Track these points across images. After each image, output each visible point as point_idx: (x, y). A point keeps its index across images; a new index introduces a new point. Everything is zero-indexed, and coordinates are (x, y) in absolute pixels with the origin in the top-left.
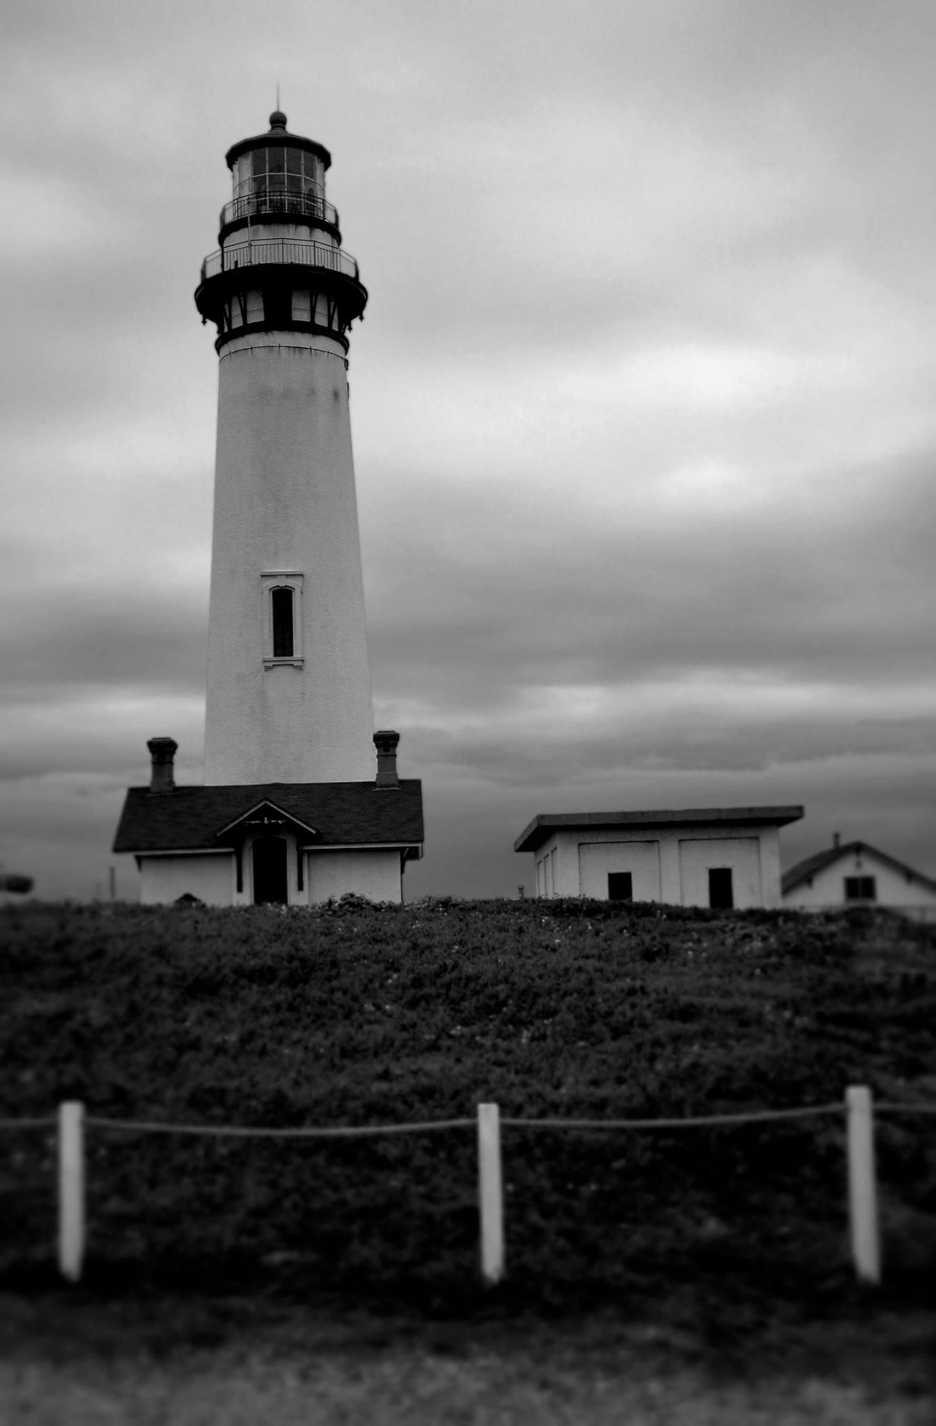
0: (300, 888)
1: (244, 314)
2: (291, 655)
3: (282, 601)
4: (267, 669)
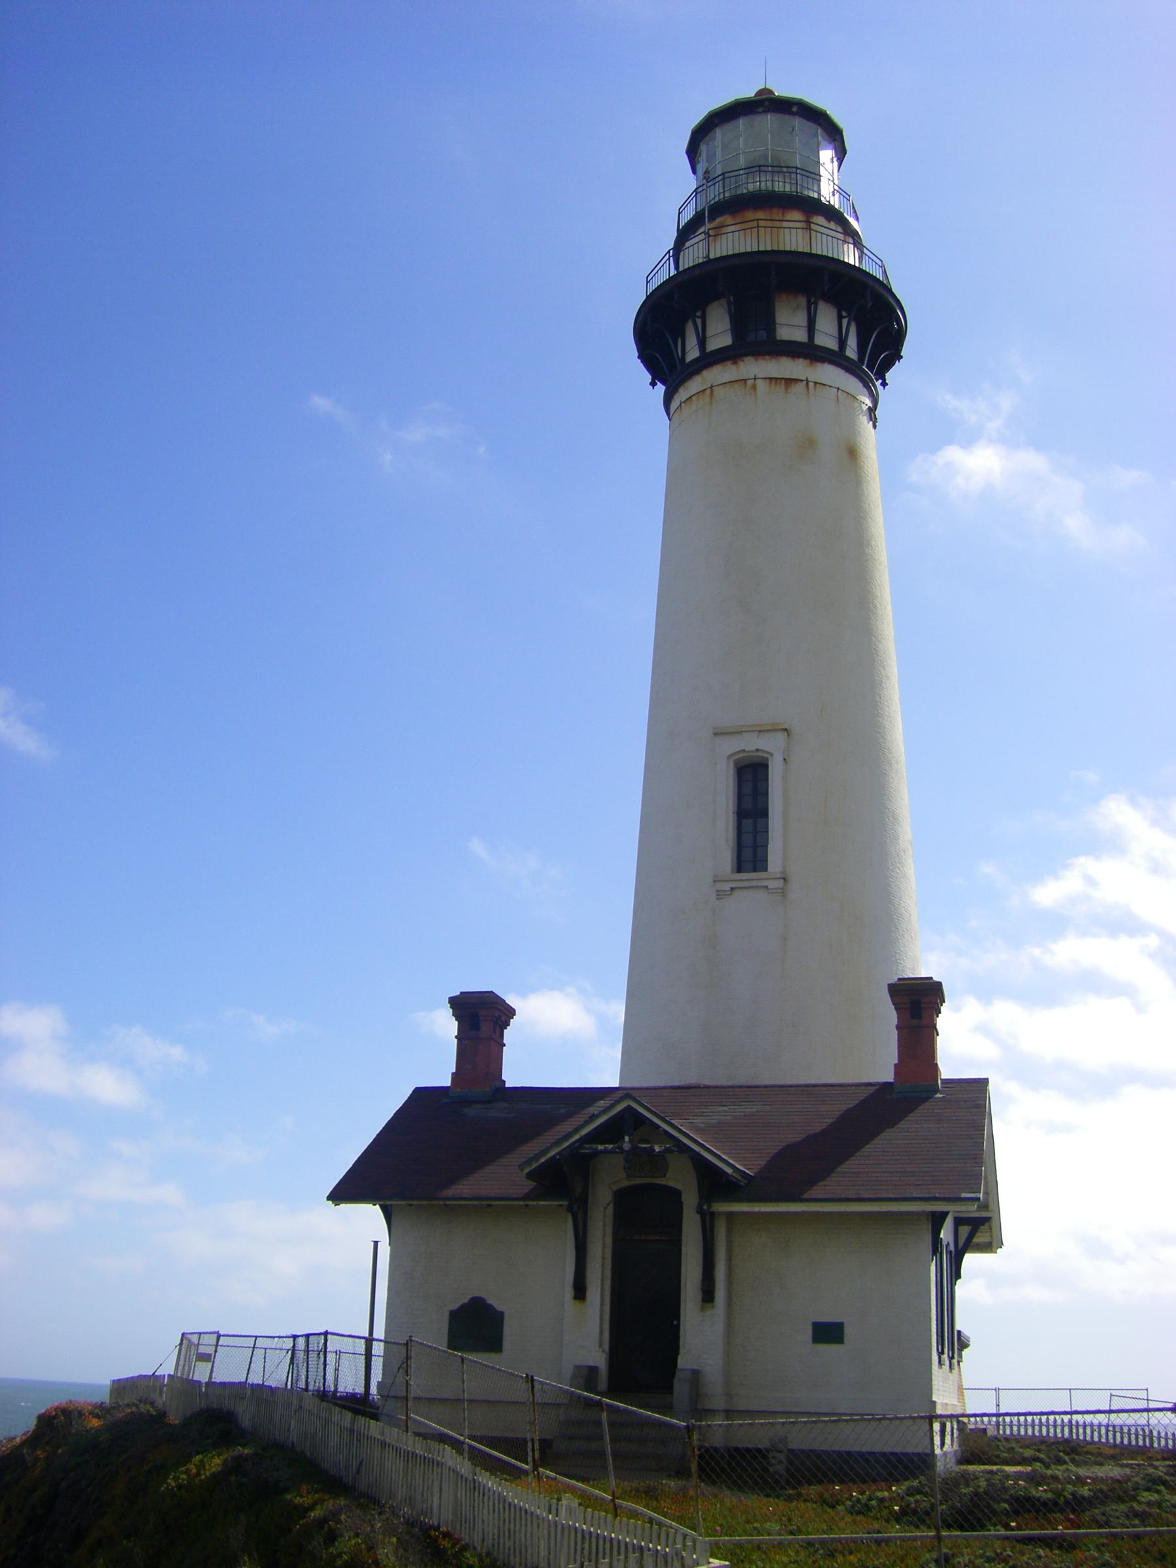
0: (708, 1295)
1: (702, 342)
2: (765, 869)
3: (752, 776)
4: (720, 895)
